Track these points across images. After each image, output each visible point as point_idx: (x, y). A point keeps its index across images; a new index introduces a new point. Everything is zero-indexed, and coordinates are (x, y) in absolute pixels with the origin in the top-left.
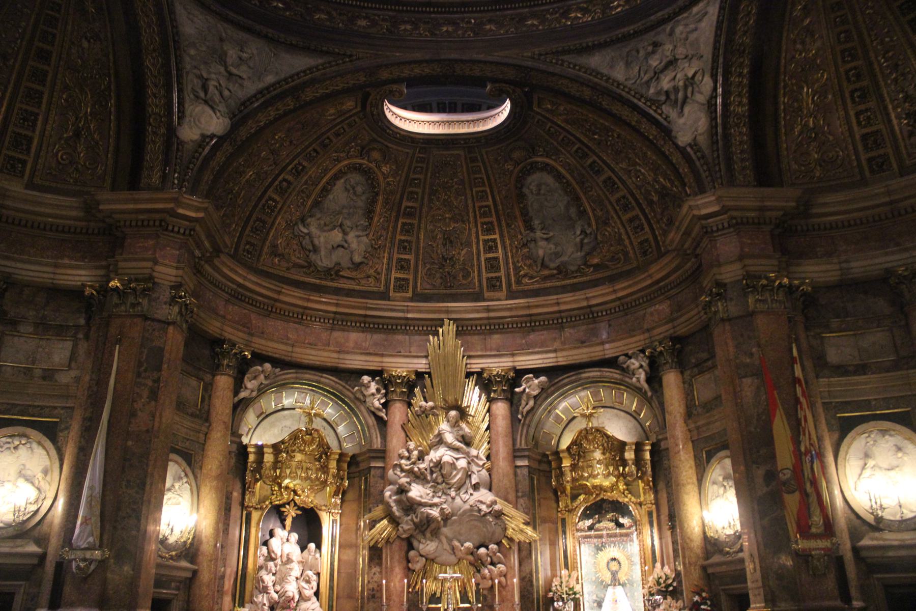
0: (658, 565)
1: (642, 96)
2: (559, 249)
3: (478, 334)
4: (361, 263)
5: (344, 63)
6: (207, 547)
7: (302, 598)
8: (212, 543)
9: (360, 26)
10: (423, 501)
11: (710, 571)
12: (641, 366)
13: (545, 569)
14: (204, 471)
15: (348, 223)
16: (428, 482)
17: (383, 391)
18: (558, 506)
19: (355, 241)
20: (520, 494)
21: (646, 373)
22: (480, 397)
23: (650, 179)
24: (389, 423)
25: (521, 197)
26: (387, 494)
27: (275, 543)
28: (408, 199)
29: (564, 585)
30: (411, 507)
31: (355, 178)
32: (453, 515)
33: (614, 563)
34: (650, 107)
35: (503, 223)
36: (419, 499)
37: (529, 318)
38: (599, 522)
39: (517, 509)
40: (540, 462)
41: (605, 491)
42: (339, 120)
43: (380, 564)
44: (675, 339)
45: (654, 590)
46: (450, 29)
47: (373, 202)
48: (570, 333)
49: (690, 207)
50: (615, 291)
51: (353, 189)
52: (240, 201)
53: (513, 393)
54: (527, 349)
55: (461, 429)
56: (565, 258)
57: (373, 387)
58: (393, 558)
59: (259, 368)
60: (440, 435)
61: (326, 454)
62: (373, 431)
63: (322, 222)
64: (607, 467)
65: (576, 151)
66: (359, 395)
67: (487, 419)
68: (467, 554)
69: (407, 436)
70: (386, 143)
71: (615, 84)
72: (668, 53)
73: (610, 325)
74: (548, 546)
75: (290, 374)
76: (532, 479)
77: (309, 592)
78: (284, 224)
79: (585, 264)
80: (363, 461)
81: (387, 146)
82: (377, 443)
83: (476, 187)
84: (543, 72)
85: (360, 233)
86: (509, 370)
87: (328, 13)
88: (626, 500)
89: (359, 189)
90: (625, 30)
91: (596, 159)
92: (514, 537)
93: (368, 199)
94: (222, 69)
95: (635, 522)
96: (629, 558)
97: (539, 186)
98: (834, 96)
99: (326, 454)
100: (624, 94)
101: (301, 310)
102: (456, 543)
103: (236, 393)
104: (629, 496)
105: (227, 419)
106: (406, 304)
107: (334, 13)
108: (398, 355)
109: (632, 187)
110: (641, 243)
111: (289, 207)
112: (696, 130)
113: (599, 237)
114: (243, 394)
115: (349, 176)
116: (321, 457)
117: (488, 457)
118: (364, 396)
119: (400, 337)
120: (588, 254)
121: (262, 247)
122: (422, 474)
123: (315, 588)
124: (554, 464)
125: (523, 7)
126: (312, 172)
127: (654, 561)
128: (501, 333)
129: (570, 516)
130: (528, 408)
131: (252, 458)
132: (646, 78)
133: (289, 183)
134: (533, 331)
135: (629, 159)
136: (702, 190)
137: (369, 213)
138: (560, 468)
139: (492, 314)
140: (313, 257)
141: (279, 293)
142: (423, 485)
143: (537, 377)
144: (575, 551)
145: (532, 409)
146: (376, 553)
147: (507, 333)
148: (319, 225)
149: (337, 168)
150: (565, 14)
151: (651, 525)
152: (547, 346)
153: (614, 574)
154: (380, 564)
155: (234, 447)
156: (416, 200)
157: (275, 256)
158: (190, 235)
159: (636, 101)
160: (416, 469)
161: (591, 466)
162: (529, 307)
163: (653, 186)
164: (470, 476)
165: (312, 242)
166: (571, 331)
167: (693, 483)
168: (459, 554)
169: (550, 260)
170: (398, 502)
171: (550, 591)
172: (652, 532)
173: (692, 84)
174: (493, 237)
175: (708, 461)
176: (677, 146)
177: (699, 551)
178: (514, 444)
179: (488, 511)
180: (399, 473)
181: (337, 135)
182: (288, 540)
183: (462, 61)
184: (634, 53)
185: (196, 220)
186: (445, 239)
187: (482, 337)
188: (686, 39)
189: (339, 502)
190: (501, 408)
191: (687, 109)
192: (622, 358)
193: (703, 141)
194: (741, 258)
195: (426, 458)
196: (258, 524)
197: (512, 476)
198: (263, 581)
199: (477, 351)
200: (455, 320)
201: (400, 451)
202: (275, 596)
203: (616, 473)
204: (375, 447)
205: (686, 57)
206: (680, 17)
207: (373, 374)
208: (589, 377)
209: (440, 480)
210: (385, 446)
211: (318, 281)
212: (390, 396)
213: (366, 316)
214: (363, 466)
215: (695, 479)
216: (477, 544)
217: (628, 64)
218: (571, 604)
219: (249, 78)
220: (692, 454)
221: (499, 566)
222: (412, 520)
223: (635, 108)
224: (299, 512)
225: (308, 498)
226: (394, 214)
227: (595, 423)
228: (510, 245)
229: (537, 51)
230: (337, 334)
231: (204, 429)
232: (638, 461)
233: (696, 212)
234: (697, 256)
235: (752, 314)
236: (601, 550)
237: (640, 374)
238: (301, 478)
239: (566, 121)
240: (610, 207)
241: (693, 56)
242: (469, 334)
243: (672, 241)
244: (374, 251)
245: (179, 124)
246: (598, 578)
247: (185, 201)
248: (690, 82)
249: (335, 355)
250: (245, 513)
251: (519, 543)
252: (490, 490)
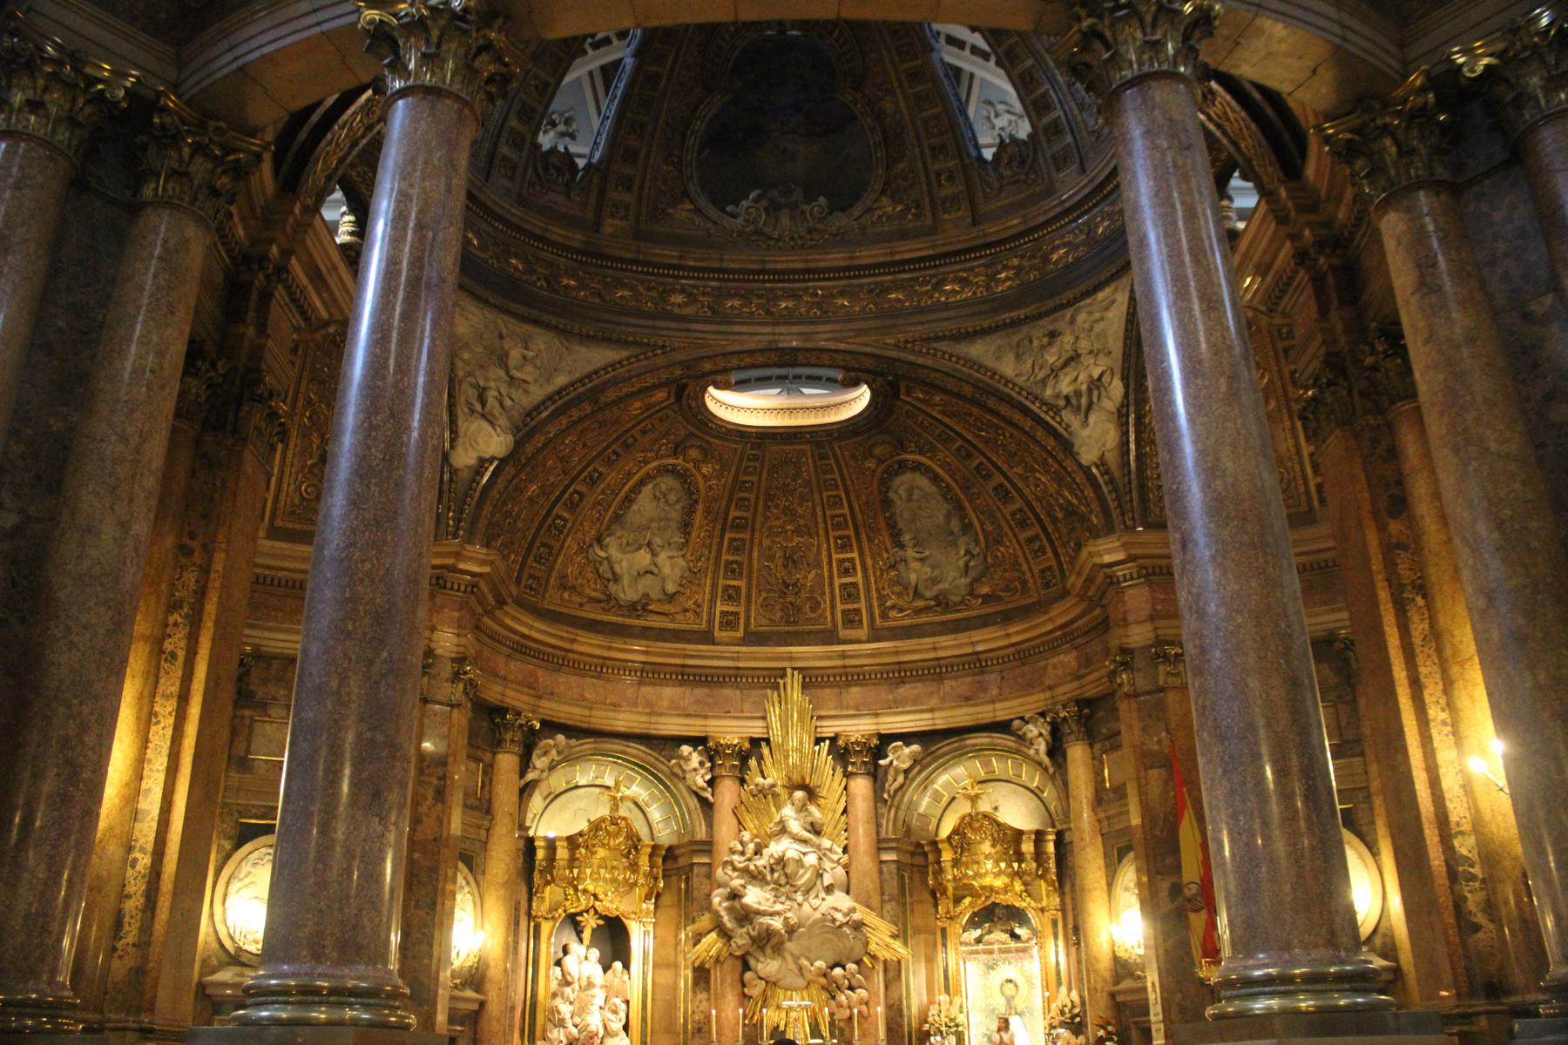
0: (1064, 989)
1: (1036, 398)
2: (937, 572)
3: (831, 687)
4: (675, 594)
5: (655, 356)
6: (495, 972)
7: (608, 1033)
8: (501, 967)
9: (674, 304)
10: (762, 908)
11: (1120, 998)
12: (1041, 735)
13: (919, 995)
14: (488, 877)
15: (658, 541)
16: (768, 883)
17: (708, 765)
18: (937, 912)
19: (668, 563)
20: (886, 898)
21: (1047, 744)
22: (834, 770)
23: (1052, 490)
24: (716, 807)
25: (887, 503)
26: (716, 900)
27: (569, 961)
28: (736, 508)
29: (942, 1015)
30: (745, 916)
31: (667, 482)
32: (799, 927)
33: (1010, 986)
34: (1046, 413)
35: (863, 537)
36: (756, 906)
37: (897, 667)
38: (990, 932)
39: (882, 917)
40: (913, 854)
41: (997, 893)
42: (646, 415)
43: (708, 989)
44: (1083, 703)
45: (1055, 1023)
46: (790, 304)
47: (690, 512)
48: (952, 687)
49: (1090, 554)
50: (1008, 635)
51: (665, 496)
52: (520, 525)
53: (877, 766)
54: (895, 706)
55: (810, 814)
56: (946, 586)
57: (695, 759)
58: (723, 979)
59: (551, 742)
60: (782, 822)
61: (636, 848)
62: (695, 816)
63: (624, 541)
64: (997, 862)
65: (958, 449)
66: (677, 770)
67: (844, 798)
68: (818, 975)
69: (740, 823)
70: (707, 438)
71: (1003, 381)
72: (1068, 347)
73: (1002, 678)
74: (923, 964)
75: (588, 744)
76: (902, 877)
77: (617, 1026)
78: (575, 547)
79: (971, 594)
80: (683, 855)
81: (708, 442)
82: (701, 833)
83: (826, 490)
84: (911, 363)
85: (675, 553)
86: (872, 735)
87: (633, 288)
88: (1024, 904)
89: (672, 497)
90: (1014, 314)
91: (984, 460)
92: (879, 954)
93: (683, 508)
94: (502, 374)
95: (1035, 932)
96: (1028, 980)
97: (910, 491)
98: (1278, 401)
99: (636, 848)
100: (1014, 394)
101: (601, 661)
102: (804, 962)
103: (522, 774)
104: (1028, 899)
105: (514, 810)
106: (737, 649)
107: (641, 289)
108: (727, 714)
110: (1042, 571)
111: (582, 524)
112: (1104, 445)
113: (989, 560)
114: (530, 776)
115: (659, 480)
116: (629, 852)
117: (845, 850)
118: (684, 771)
119: (728, 692)
120: (975, 580)
121: (548, 581)
122: (760, 873)
123: (624, 1021)
124: (931, 857)
125: (884, 274)
126: (612, 477)
127: (1059, 983)
128: (862, 685)
129: (953, 923)
130: (896, 785)
131: (540, 854)
132: (1041, 375)
133: (582, 496)
134: (903, 683)
135: (1026, 463)
136: (1110, 529)
137: (685, 527)
138: (939, 863)
139: (849, 662)
140: (613, 588)
141: (573, 641)
142: (761, 887)
143: (908, 744)
144: (958, 970)
145: (902, 786)
146: (701, 975)
147: (865, 685)
148: (621, 545)
149: (644, 470)
150: (938, 286)
151: (1056, 937)
152: (922, 704)
153: (1009, 1000)
154: (708, 989)
155: (521, 844)
156: (748, 508)
157: (565, 589)
158: (472, 592)
159: (1028, 404)
160: (752, 867)
161: (978, 863)
162: (897, 653)
163: (1057, 500)
164: (822, 875)
165: (612, 568)
166: (953, 683)
167: (1101, 889)
168: (809, 976)
169: (926, 587)
170: (730, 910)
171: (926, 1022)
172: (1056, 946)
173: (1098, 388)
174: (850, 555)
175: (1120, 861)
176: (1080, 465)
177: (1107, 975)
178: (878, 833)
179: (845, 921)
180: (730, 872)
181: (644, 432)
182: (586, 958)
183: (807, 350)
184: (1026, 343)
185: (480, 575)
186: (786, 558)
187: (836, 690)
188: (1091, 329)
189: (652, 907)
190: (861, 786)
191: (1092, 418)
192: (1016, 723)
193: (1112, 459)
194: (1151, 618)
195: (765, 852)
196: (549, 938)
197: (875, 876)
198: (559, 1013)
199: (830, 709)
200: (800, 669)
201: (732, 845)
202: (575, 1031)
203: (1010, 870)
204: (698, 837)
205: (1091, 352)
206: (1082, 303)
207: (697, 741)
208: (976, 745)
209: (783, 880)
210: (712, 837)
211: (620, 620)
212: (718, 771)
213: (684, 666)
214: (682, 861)
215: (1103, 883)
216: (831, 963)
217: (1018, 357)
218: (953, 1039)
219: (536, 380)
220: (1101, 854)
221: (859, 991)
222: (748, 933)
223: (1027, 412)
224: (601, 922)
225: (612, 904)
226: (719, 527)
227: (984, 806)
228: (874, 566)
229: (902, 337)
230: (647, 690)
231: (486, 823)
232: (1039, 855)
233: (1097, 560)
234: (1103, 606)
235: (1162, 690)
236: (993, 969)
237: (1039, 744)
238: (605, 880)
239: (944, 413)
240: (1002, 521)
241: (1099, 352)
242: (821, 688)
243: (1073, 585)
244: (691, 578)
245: (452, 447)
246: (989, 1005)
247: (465, 553)
248: (1096, 384)
249: (644, 718)
250: (532, 924)
251: (885, 962)
252: (848, 893)
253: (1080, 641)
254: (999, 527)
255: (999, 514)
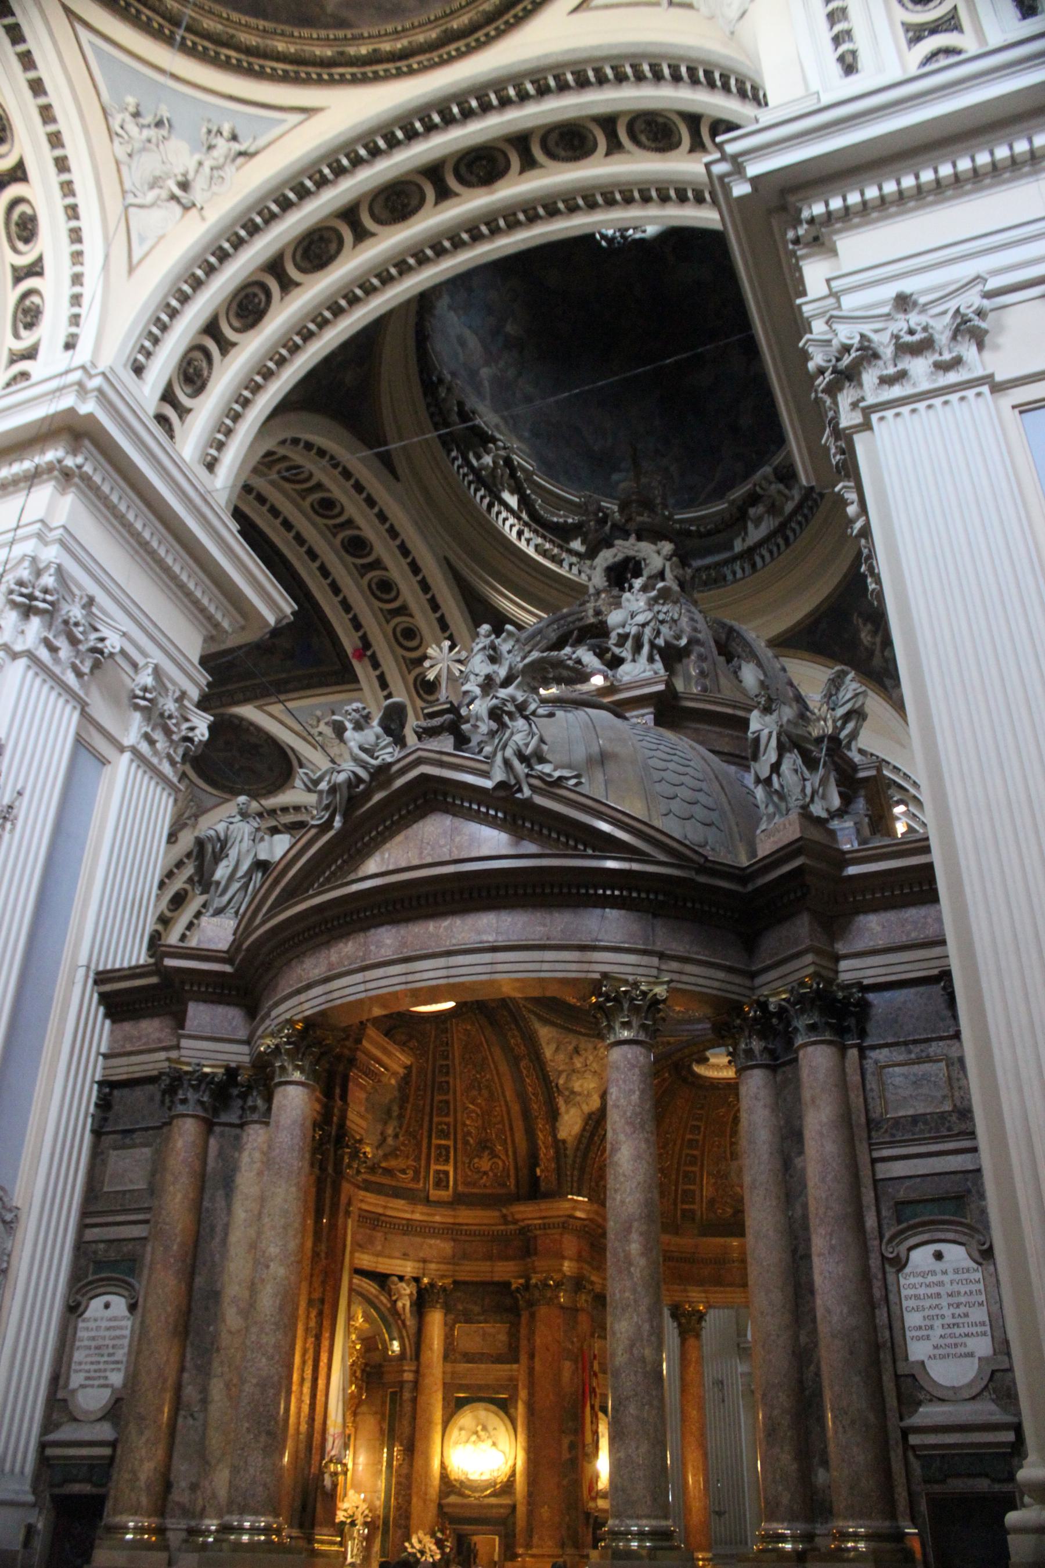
12: (411, 1294)
109: (459, 1117)
193: (570, 1139)
217: (557, 1049)
235: (577, 1310)
253: (463, 1238)
254: (421, 1126)
255: (427, 1119)
